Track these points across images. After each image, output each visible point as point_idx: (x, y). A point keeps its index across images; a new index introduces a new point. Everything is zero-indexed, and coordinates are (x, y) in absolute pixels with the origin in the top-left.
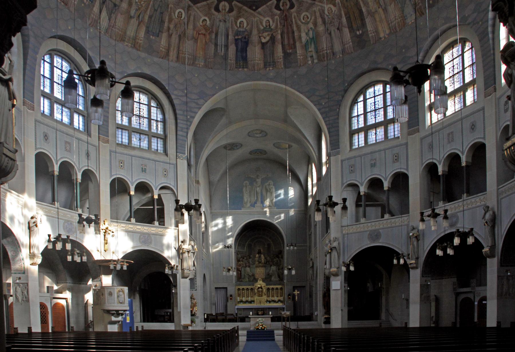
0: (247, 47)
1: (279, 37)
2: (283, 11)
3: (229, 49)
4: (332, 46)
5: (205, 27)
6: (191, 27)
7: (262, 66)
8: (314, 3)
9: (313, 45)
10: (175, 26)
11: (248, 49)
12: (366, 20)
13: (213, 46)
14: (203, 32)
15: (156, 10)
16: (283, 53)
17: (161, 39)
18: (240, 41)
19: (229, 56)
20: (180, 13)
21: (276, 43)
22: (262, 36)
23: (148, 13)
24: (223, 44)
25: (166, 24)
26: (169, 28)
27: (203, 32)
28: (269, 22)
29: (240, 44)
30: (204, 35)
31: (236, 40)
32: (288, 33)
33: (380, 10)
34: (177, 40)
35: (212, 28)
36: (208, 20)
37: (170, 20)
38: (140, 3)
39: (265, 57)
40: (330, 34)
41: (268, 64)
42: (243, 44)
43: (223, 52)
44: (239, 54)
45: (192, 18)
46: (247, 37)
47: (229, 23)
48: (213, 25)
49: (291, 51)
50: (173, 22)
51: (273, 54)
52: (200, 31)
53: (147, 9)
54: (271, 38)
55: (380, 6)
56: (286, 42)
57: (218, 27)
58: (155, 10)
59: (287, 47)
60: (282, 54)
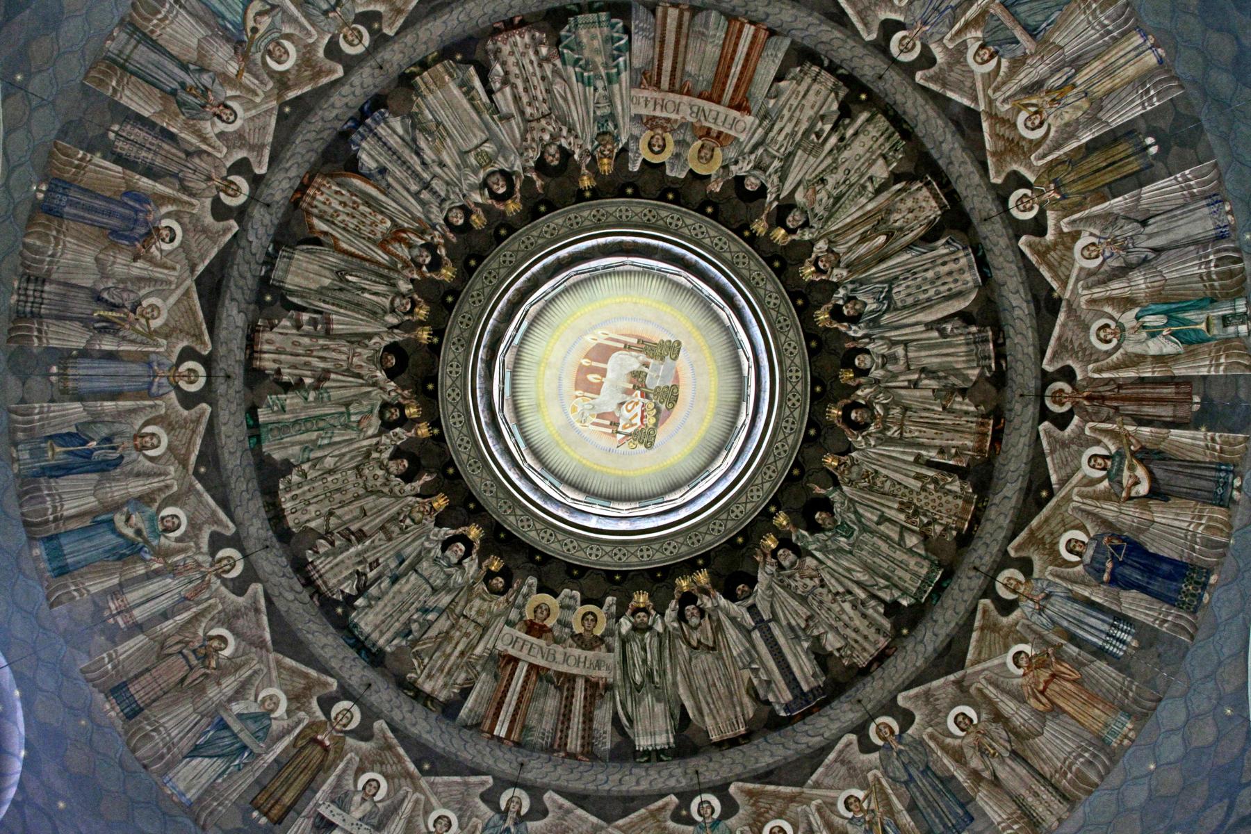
0: (1146, 552)
1: (1146, 430)
2: (1075, 404)
3: (1131, 614)
4: (1195, 243)
5: (1036, 664)
6: (1008, 706)
7: (1219, 514)
8: (1068, 301)
9: (1191, 315)
10: (982, 752)
11: (1152, 550)
12: (1114, 125)
13: (1102, 665)
14: (1044, 675)
15: (906, 783)
16: (1197, 428)
17: (985, 814)
18: (1120, 569)
19: (1149, 621)
20: (960, 719)
21: (1161, 447)
22: (1130, 489)
23: (900, 807)
24: (1105, 627)
25: (960, 776)
26: (976, 776)
27: (1044, 675)
28: (1095, 456)
29: (1127, 571)
30: (1053, 676)
31: (1113, 581)
32: (1140, 400)
33: (1079, 80)
34: (1022, 771)
35: (1048, 644)
36: (1021, 647)
37: (958, 756)
38: (861, 810)
39: (1195, 497)
40: (1158, 251)
41: (1219, 491)
42: (1131, 562)
43: (1128, 638)
44: (1156, 586)
45: (991, 691)
46: (1116, 542)
47: (1056, 585)
48: (1041, 637)
49: (1196, 399)
50: (969, 753)
51: (1195, 464)
52: (1037, 683)
53: (888, 803)
54: (1141, 461)
55: (1069, 84)
56: (1166, 412)
57: (1053, 622)
58: (906, 783)
59: (1182, 412)
60: (1200, 434)
